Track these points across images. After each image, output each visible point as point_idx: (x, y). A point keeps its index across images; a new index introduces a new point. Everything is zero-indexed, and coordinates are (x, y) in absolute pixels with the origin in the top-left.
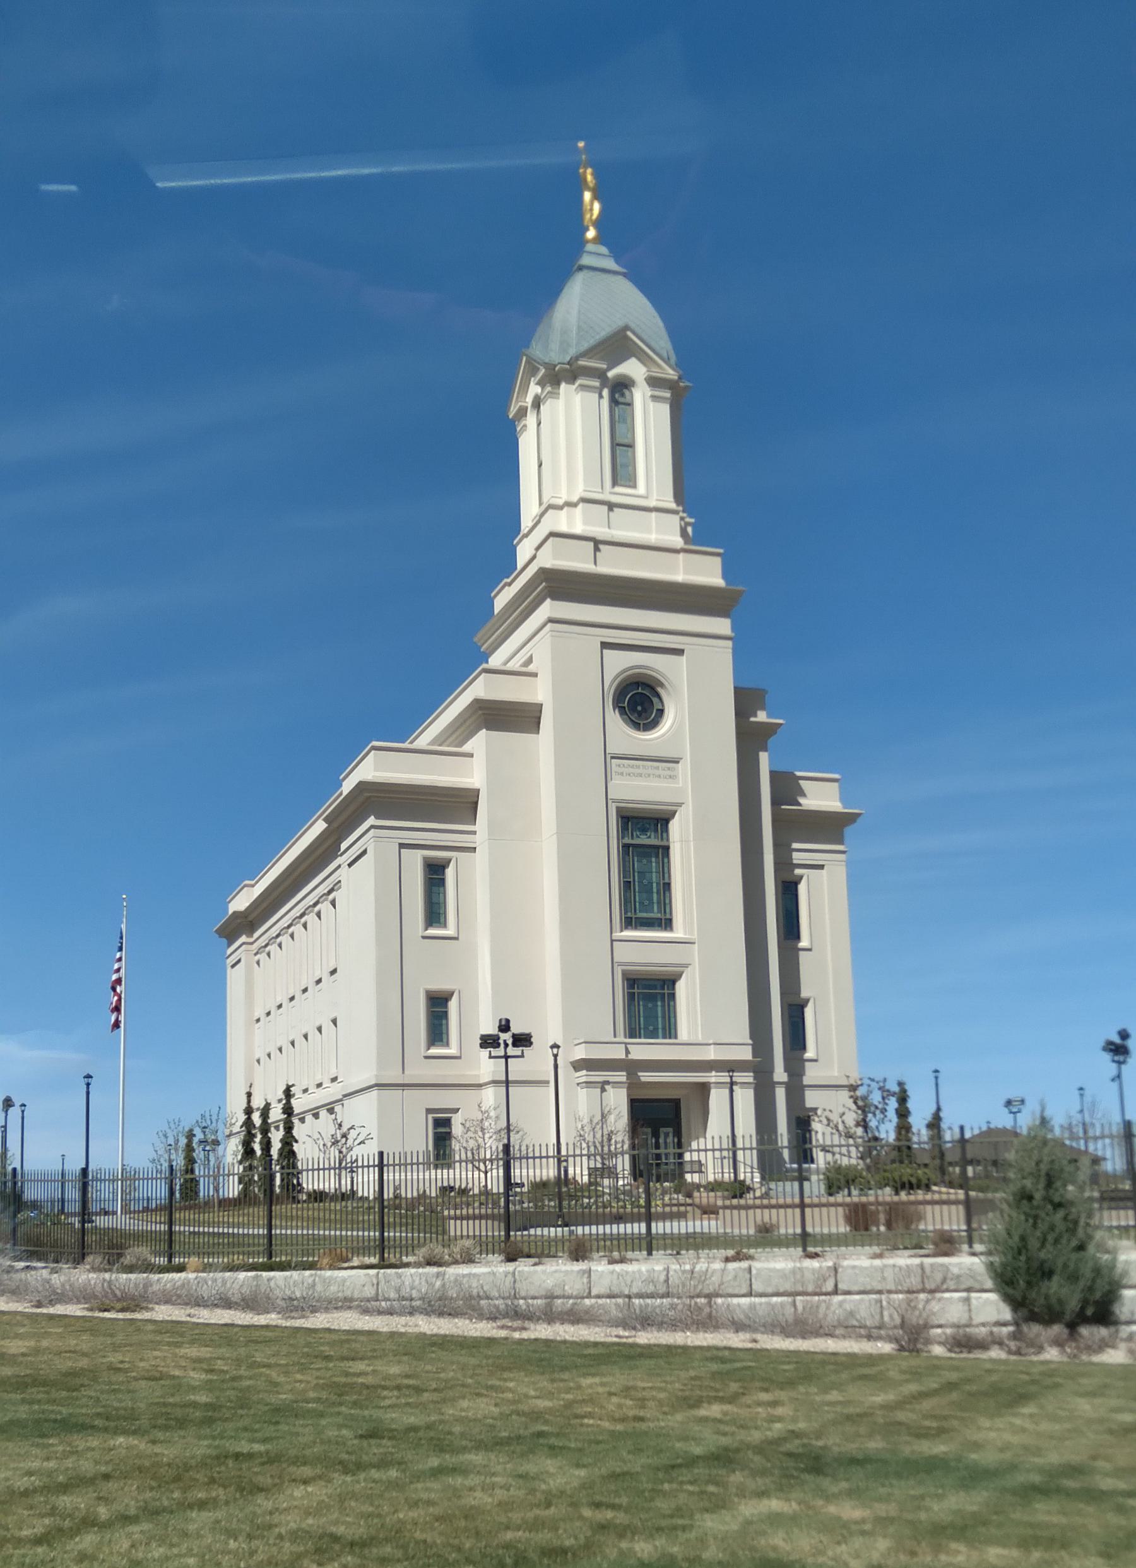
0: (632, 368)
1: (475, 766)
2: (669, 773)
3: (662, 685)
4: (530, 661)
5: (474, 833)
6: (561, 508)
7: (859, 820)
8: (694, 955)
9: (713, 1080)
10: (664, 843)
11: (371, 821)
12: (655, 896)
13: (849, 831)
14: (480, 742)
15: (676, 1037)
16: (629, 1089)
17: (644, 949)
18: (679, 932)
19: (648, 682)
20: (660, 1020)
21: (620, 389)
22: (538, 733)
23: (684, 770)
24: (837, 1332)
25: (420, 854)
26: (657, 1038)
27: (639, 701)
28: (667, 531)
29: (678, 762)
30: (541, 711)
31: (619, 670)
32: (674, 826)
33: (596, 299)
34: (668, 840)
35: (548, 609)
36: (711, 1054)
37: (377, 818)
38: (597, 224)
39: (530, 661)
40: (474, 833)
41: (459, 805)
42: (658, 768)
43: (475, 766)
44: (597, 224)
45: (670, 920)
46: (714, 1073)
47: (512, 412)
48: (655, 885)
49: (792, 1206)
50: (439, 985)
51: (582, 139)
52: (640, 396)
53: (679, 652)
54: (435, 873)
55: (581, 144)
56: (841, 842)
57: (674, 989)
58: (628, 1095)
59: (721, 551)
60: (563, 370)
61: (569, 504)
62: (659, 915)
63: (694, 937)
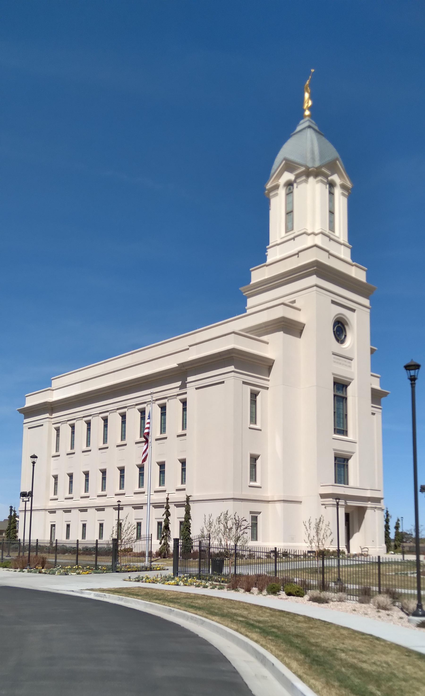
0: (335, 178)
1: (272, 347)
2: (349, 364)
3: (347, 324)
4: (294, 302)
5: (268, 380)
6: (309, 235)
7: (388, 395)
8: (356, 448)
9: (369, 506)
10: (344, 396)
11: (232, 368)
12: (341, 420)
13: (383, 400)
14: (279, 336)
15: (348, 484)
16: (345, 508)
17: (341, 445)
18: (351, 437)
19: (342, 322)
20: (342, 476)
21: (332, 185)
22: (300, 338)
23: (354, 363)
24: (303, 619)
25: (249, 388)
26: (341, 484)
27: (340, 329)
28: (345, 253)
29: (352, 360)
30: (304, 328)
31: (339, 313)
32: (349, 388)
33: (304, 144)
34: (346, 394)
35: (313, 280)
36: (368, 494)
37: (235, 368)
38: (310, 109)
39: (294, 302)
40: (268, 380)
41: (264, 366)
42: (346, 361)
43: (272, 347)
44: (310, 109)
45: (347, 431)
46: (369, 503)
47: (269, 185)
48: (341, 415)
49: (383, 563)
50: (256, 452)
51: (313, 68)
52: (338, 191)
53: (353, 310)
54: (254, 395)
55: (313, 70)
56: (380, 405)
57: (255, 462)
58: (345, 511)
59: (366, 269)
60: (312, 171)
61: (313, 234)
62: (342, 429)
63: (357, 440)
